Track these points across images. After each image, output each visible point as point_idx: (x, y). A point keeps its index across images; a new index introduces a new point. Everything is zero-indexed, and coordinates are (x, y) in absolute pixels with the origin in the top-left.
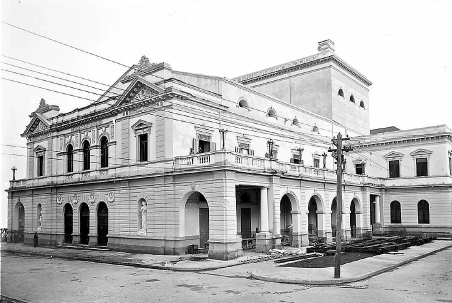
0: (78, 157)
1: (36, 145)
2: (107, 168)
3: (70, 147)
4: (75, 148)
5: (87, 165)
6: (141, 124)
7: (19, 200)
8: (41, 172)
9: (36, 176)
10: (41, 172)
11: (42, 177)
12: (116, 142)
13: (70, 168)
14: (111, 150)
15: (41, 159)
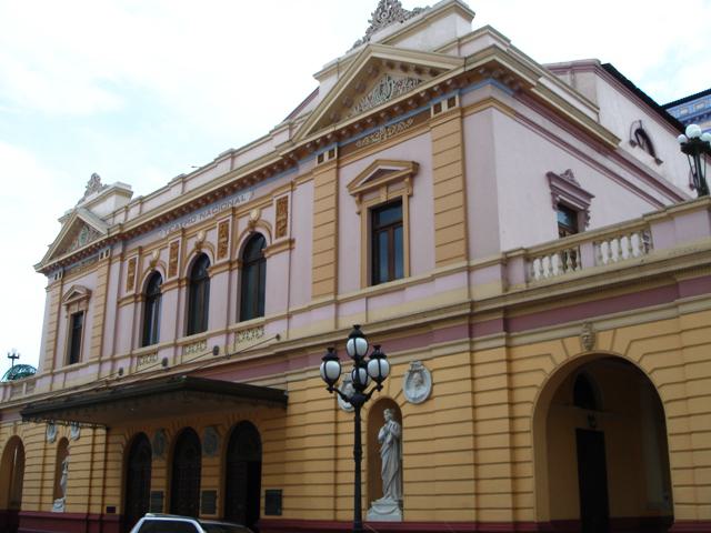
0: (172, 304)
1: (67, 288)
2: (260, 320)
3: (155, 276)
4: (166, 279)
5: (195, 319)
6: (381, 173)
7: (15, 430)
8: (74, 355)
9: (60, 366)
10: (74, 355)
11: (76, 365)
12: (291, 242)
13: (148, 333)
14: (275, 266)
15: (77, 321)
